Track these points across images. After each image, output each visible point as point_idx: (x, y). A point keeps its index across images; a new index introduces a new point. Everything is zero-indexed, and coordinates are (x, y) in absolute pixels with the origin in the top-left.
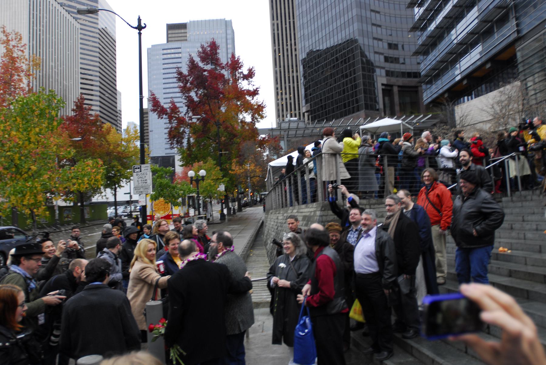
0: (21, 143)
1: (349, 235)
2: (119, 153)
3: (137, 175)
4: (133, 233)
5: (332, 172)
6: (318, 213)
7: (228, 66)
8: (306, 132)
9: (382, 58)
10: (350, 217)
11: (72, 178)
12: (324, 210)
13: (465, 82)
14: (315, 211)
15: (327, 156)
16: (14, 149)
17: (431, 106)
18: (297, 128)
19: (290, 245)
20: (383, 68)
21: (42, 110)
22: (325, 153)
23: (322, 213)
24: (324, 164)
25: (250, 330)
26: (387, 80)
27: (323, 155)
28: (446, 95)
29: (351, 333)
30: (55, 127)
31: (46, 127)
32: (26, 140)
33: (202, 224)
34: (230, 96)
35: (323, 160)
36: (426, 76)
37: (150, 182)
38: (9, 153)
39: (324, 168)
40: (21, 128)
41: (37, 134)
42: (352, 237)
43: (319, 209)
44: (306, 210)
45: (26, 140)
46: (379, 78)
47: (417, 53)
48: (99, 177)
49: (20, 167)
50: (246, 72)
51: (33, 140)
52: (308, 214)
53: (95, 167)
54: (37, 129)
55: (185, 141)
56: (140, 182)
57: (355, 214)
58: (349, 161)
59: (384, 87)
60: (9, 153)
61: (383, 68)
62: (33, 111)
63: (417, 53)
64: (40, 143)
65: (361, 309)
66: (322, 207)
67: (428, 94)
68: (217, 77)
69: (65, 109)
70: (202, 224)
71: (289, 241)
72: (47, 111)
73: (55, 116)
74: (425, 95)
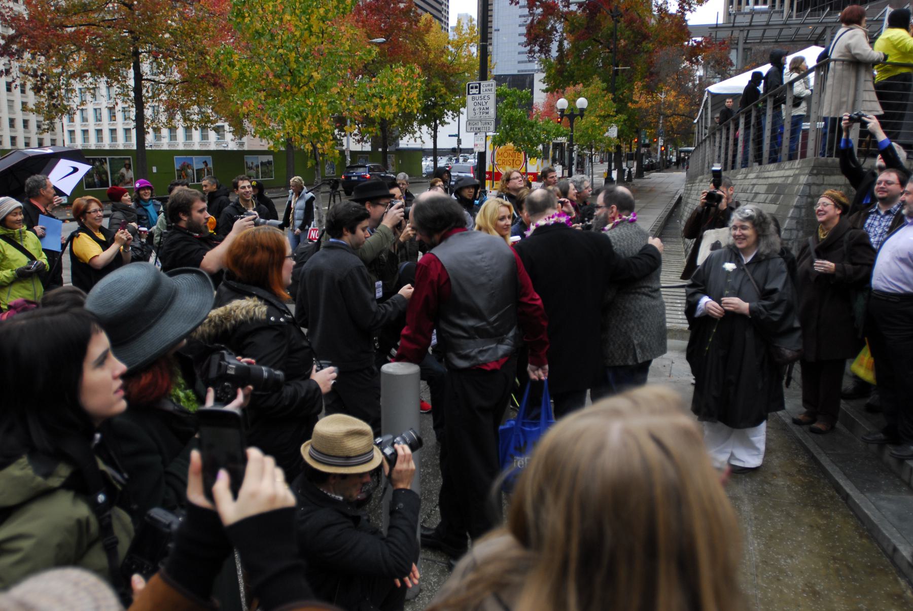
0: (298, 33)
1: (869, 221)
2: (443, 65)
3: (473, 99)
4: (468, 187)
5: (844, 99)
6: (803, 179)
8: (784, 32)
10: (876, 187)
11: (374, 95)
12: (816, 175)
14: (796, 176)
15: (839, 67)
18: (767, 25)
19: (748, 232)
22: (835, 60)
23: (812, 179)
24: (829, 82)
25: (656, 363)
27: (832, 64)
29: (842, 401)
32: (306, 30)
33: (582, 182)
35: (830, 74)
37: (492, 111)
38: (281, 51)
39: (828, 91)
41: (323, 19)
42: (875, 226)
43: (807, 171)
44: (777, 173)
45: (306, 30)
48: (414, 95)
51: (315, 29)
52: (779, 181)
54: (322, 11)
55: (554, 46)
56: (477, 111)
57: (887, 183)
58: (889, 79)
60: (281, 51)
64: (325, 35)
65: (872, 360)
66: (814, 168)
70: (582, 182)
71: (747, 224)
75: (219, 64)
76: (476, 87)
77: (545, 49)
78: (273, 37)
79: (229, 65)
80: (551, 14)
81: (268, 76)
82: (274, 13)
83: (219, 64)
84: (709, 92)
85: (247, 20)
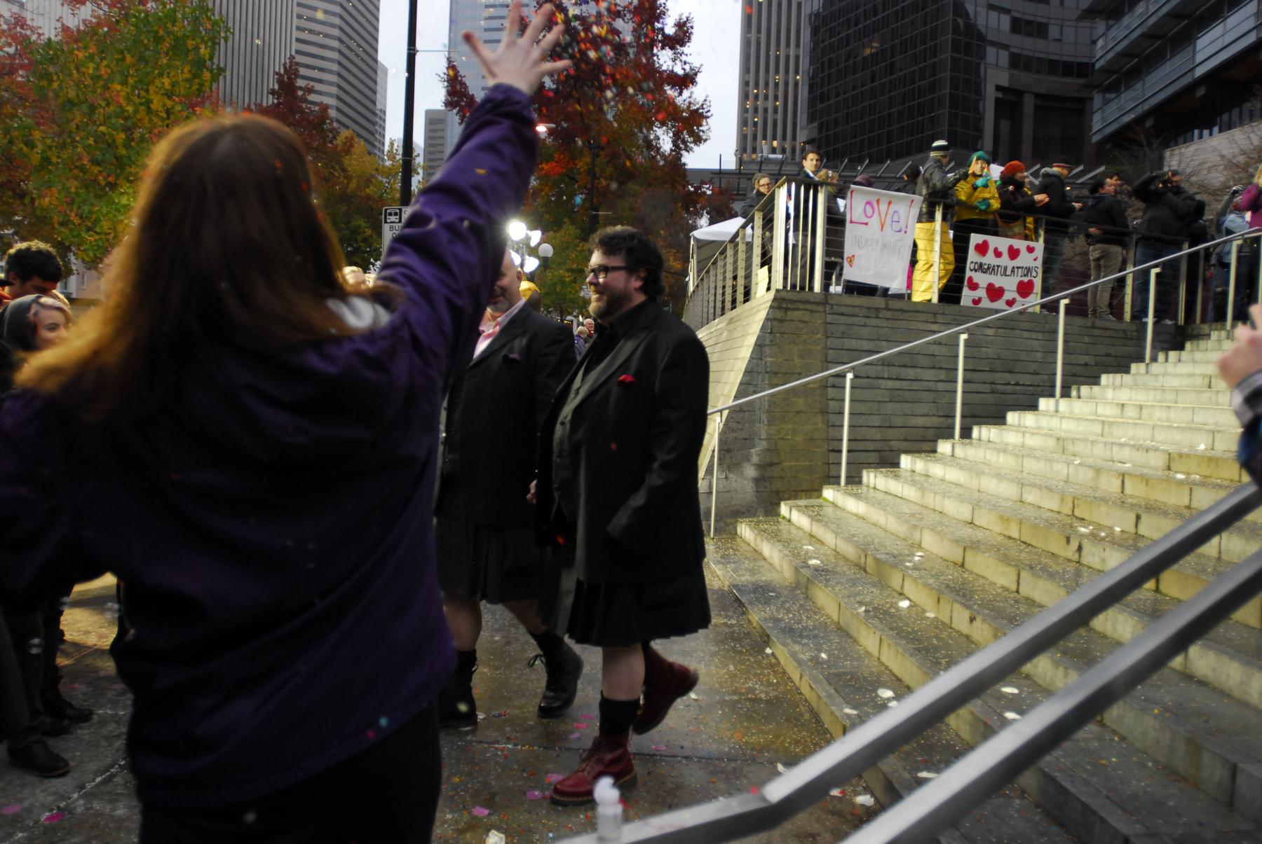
0: (130, 109)
7: (630, 12)
9: (1006, 20)
13: (1201, 92)
16: (113, 121)
17: (1108, 146)
20: (1006, 47)
21: (177, 39)
26: (1011, 77)
28: (1149, 123)
30: (207, 84)
31: (187, 80)
32: (141, 104)
36: (1106, 70)
38: (102, 129)
40: (132, 76)
45: (141, 104)
46: (990, 72)
47: (1090, 13)
49: (126, 160)
50: (670, 30)
51: (156, 105)
54: (166, 81)
59: (1000, 95)
60: (102, 129)
61: (1006, 47)
62: (158, 40)
63: (1090, 13)
64: (172, 117)
67: (1107, 116)
69: (230, 43)
72: (191, 43)
73: (207, 57)
75: (11, 142)
76: (396, 214)
78: (93, 108)
79: (26, 144)
81: (80, 159)
83: (11, 142)
84: (697, 240)
85: (55, 85)
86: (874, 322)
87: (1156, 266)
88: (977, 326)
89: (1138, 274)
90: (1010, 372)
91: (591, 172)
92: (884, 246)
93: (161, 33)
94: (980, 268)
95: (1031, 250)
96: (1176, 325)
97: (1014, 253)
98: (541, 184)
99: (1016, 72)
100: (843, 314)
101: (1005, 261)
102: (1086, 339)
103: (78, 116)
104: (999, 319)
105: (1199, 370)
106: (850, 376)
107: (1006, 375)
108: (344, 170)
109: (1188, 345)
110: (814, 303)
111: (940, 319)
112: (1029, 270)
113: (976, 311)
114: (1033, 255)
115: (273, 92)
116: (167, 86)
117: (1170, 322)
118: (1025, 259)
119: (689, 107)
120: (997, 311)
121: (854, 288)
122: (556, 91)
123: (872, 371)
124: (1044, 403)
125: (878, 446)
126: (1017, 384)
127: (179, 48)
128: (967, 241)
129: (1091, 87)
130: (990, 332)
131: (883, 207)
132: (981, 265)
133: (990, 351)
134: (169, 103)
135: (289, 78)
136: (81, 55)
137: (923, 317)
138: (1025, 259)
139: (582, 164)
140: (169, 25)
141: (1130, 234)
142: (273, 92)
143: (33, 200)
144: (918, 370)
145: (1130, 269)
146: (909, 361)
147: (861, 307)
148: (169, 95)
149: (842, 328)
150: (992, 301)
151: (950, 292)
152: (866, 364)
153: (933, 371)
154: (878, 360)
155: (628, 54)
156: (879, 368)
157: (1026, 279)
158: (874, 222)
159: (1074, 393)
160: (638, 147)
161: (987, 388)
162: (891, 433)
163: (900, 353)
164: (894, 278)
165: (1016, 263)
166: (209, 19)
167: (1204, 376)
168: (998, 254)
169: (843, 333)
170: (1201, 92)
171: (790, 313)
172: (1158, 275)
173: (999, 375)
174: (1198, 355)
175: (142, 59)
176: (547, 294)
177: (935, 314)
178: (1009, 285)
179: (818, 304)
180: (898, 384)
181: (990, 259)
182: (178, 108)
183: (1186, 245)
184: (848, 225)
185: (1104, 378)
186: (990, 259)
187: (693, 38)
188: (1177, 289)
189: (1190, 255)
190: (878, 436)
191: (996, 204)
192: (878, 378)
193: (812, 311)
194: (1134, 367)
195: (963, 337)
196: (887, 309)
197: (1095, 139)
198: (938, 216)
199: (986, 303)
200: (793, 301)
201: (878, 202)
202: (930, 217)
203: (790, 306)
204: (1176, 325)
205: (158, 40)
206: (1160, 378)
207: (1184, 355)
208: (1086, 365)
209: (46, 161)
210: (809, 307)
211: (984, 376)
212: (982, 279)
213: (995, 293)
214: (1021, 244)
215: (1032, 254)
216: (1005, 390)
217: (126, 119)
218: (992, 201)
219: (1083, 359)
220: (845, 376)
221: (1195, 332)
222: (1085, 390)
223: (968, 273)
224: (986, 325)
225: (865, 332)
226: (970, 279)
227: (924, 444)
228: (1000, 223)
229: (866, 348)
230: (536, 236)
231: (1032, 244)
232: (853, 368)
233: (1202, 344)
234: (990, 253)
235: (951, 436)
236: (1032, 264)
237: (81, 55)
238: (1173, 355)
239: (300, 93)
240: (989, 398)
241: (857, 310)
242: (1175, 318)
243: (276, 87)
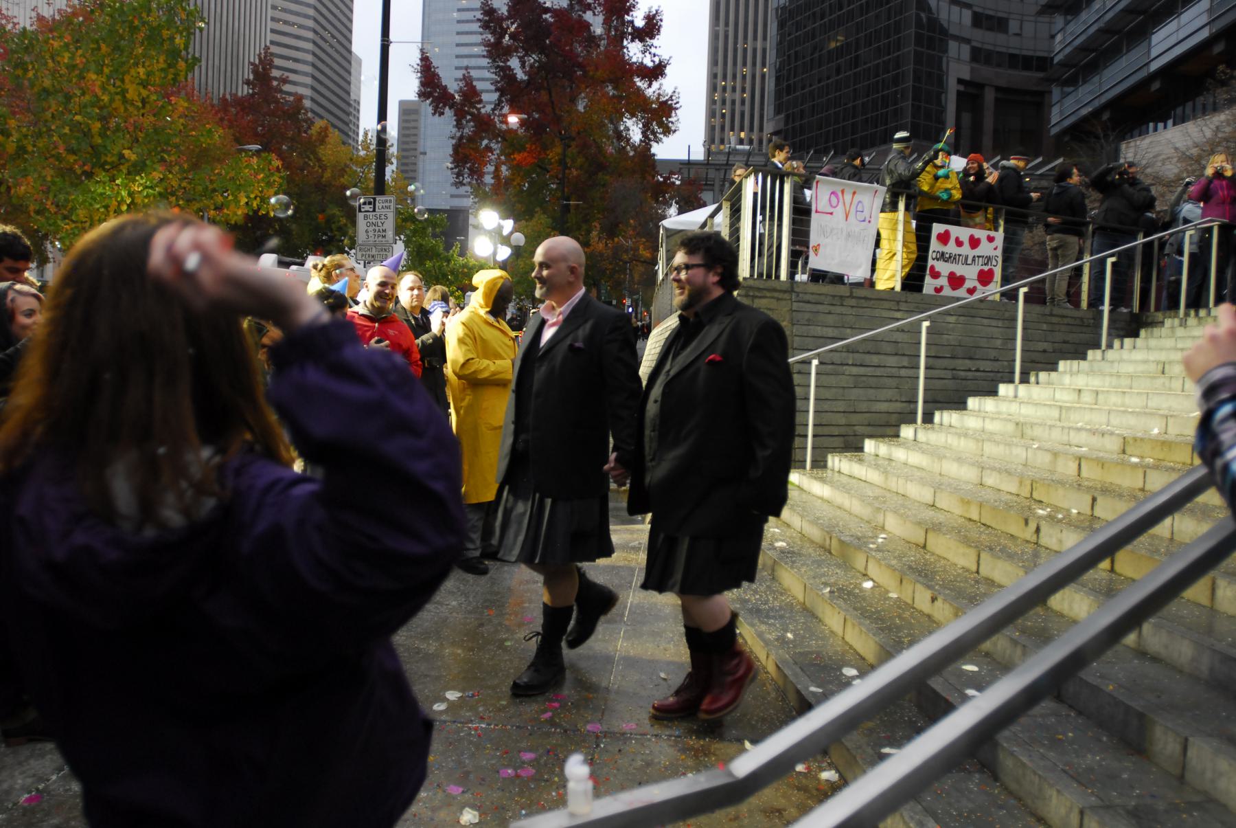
0: (106, 98)
3: (366, 217)
9: (967, 15)
11: (214, 190)
13: (1156, 86)
16: (89, 110)
17: (1066, 139)
20: (968, 41)
21: (152, 29)
26: (972, 70)
28: (1106, 116)
31: (162, 70)
34: (599, 73)
36: (1064, 64)
38: (78, 118)
40: (108, 66)
41: (144, 84)
47: (1048, 9)
49: (102, 149)
50: (640, 23)
53: (263, 170)
56: (371, 234)
59: (962, 88)
60: (78, 118)
61: (968, 41)
62: (133, 29)
64: (148, 106)
67: (1066, 109)
68: (571, 24)
74: (1055, 111)
76: (370, 203)
77: (477, 173)
78: (68, 98)
80: (486, 131)
81: (56, 147)
82: (71, 67)
84: (666, 230)
85: (31, 74)
86: (838, 309)
87: (1112, 255)
88: (939, 313)
89: (1094, 263)
90: (971, 358)
91: (562, 162)
92: (849, 235)
93: (136, 23)
94: (942, 257)
95: (991, 239)
96: (1131, 312)
97: (975, 243)
98: (513, 174)
99: (975, 65)
100: (809, 302)
101: (966, 250)
102: (1045, 327)
103: (54, 104)
104: (960, 307)
105: (1153, 356)
106: (815, 362)
107: (967, 361)
108: (319, 160)
109: (1143, 332)
110: (780, 291)
111: (903, 306)
112: (989, 259)
113: (938, 299)
114: (993, 245)
115: (248, 82)
116: (143, 76)
117: (1125, 310)
118: (985, 249)
119: (658, 98)
120: (958, 299)
121: (818, 276)
122: (529, 82)
123: (837, 358)
124: (1003, 389)
125: (843, 430)
126: (977, 370)
127: (154, 38)
128: (929, 230)
129: (1050, 81)
130: (952, 319)
131: (848, 197)
132: (943, 254)
133: (951, 338)
134: (144, 93)
135: (264, 69)
136: (56, 44)
137: (887, 305)
138: (985, 249)
139: (554, 154)
140: (144, 15)
141: (1086, 224)
142: (248, 82)
143: (9, 189)
144: (882, 357)
145: (1087, 258)
146: (873, 347)
147: (826, 295)
148: (144, 84)
149: (807, 316)
150: (954, 289)
151: (913, 281)
152: (831, 351)
153: (896, 358)
154: (843, 346)
155: (599, 46)
156: (844, 354)
157: (986, 268)
158: (839, 212)
159: (1033, 379)
160: (608, 138)
161: (949, 374)
162: (855, 418)
163: (864, 340)
164: (860, 267)
165: (977, 252)
166: (184, 9)
167: (1158, 363)
168: (959, 243)
169: (809, 320)
170: (1156, 86)
171: (756, 301)
172: (1114, 264)
173: (960, 361)
174: (1153, 342)
175: (117, 48)
176: (518, 283)
177: (898, 302)
178: (970, 273)
179: (785, 292)
180: (862, 370)
181: (951, 248)
182: (154, 97)
183: (1141, 235)
184: (813, 214)
185: (1062, 365)
186: (951, 248)
187: (662, 30)
188: (1133, 277)
189: (1145, 244)
190: (843, 421)
191: (957, 195)
192: (842, 364)
193: (778, 299)
194: (1090, 353)
195: (926, 324)
196: (851, 296)
197: (1054, 131)
198: (902, 205)
199: (947, 292)
200: (759, 289)
201: (843, 192)
202: (894, 208)
203: (757, 294)
204: (1131, 312)
205: (133, 29)
206: (1116, 365)
207: (1139, 341)
208: (1044, 351)
209: (21, 150)
210: (776, 295)
211: (946, 363)
212: (944, 268)
213: (956, 281)
214: (981, 234)
215: (992, 242)
216: (967, 375)
217: (101, 108)
218: (954, 192)
219: (1042, 346)
220: (810, 363)
221: (1149, 320)
222: (1043, 376)
223: (930, 262)
224: (947, 313)
225: (830, 319)
226: (932, 268)
227: (887, 429)
228: (962, 213)
229: (830, 335)
230: (508, 225)
231: (992, 233)
232: (818, 355)
233: (1156, 331)
234: (952, 242)
235: (914, 421)
236: (991, 253)
237: (56, 44)
238: (1127, 341)
239: (275, 83)
240: (950, 384)
241: (823, 297)
242: (1129, 304)
243: (251, 77)
